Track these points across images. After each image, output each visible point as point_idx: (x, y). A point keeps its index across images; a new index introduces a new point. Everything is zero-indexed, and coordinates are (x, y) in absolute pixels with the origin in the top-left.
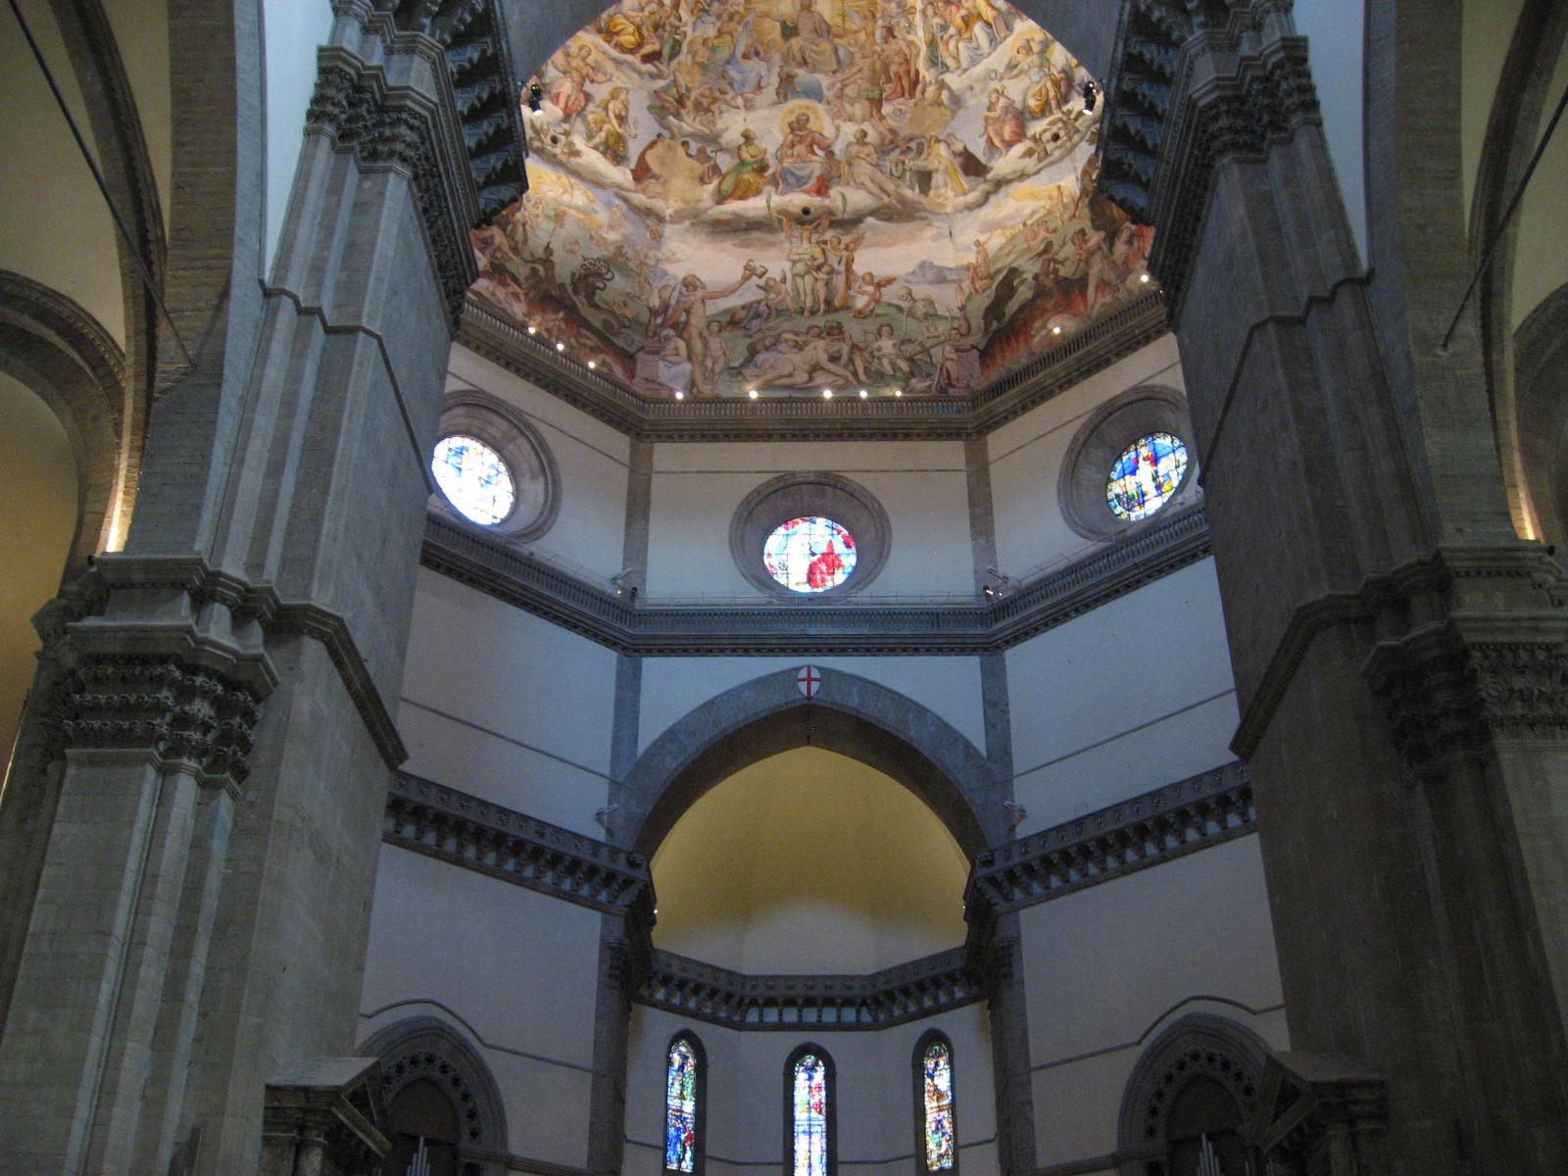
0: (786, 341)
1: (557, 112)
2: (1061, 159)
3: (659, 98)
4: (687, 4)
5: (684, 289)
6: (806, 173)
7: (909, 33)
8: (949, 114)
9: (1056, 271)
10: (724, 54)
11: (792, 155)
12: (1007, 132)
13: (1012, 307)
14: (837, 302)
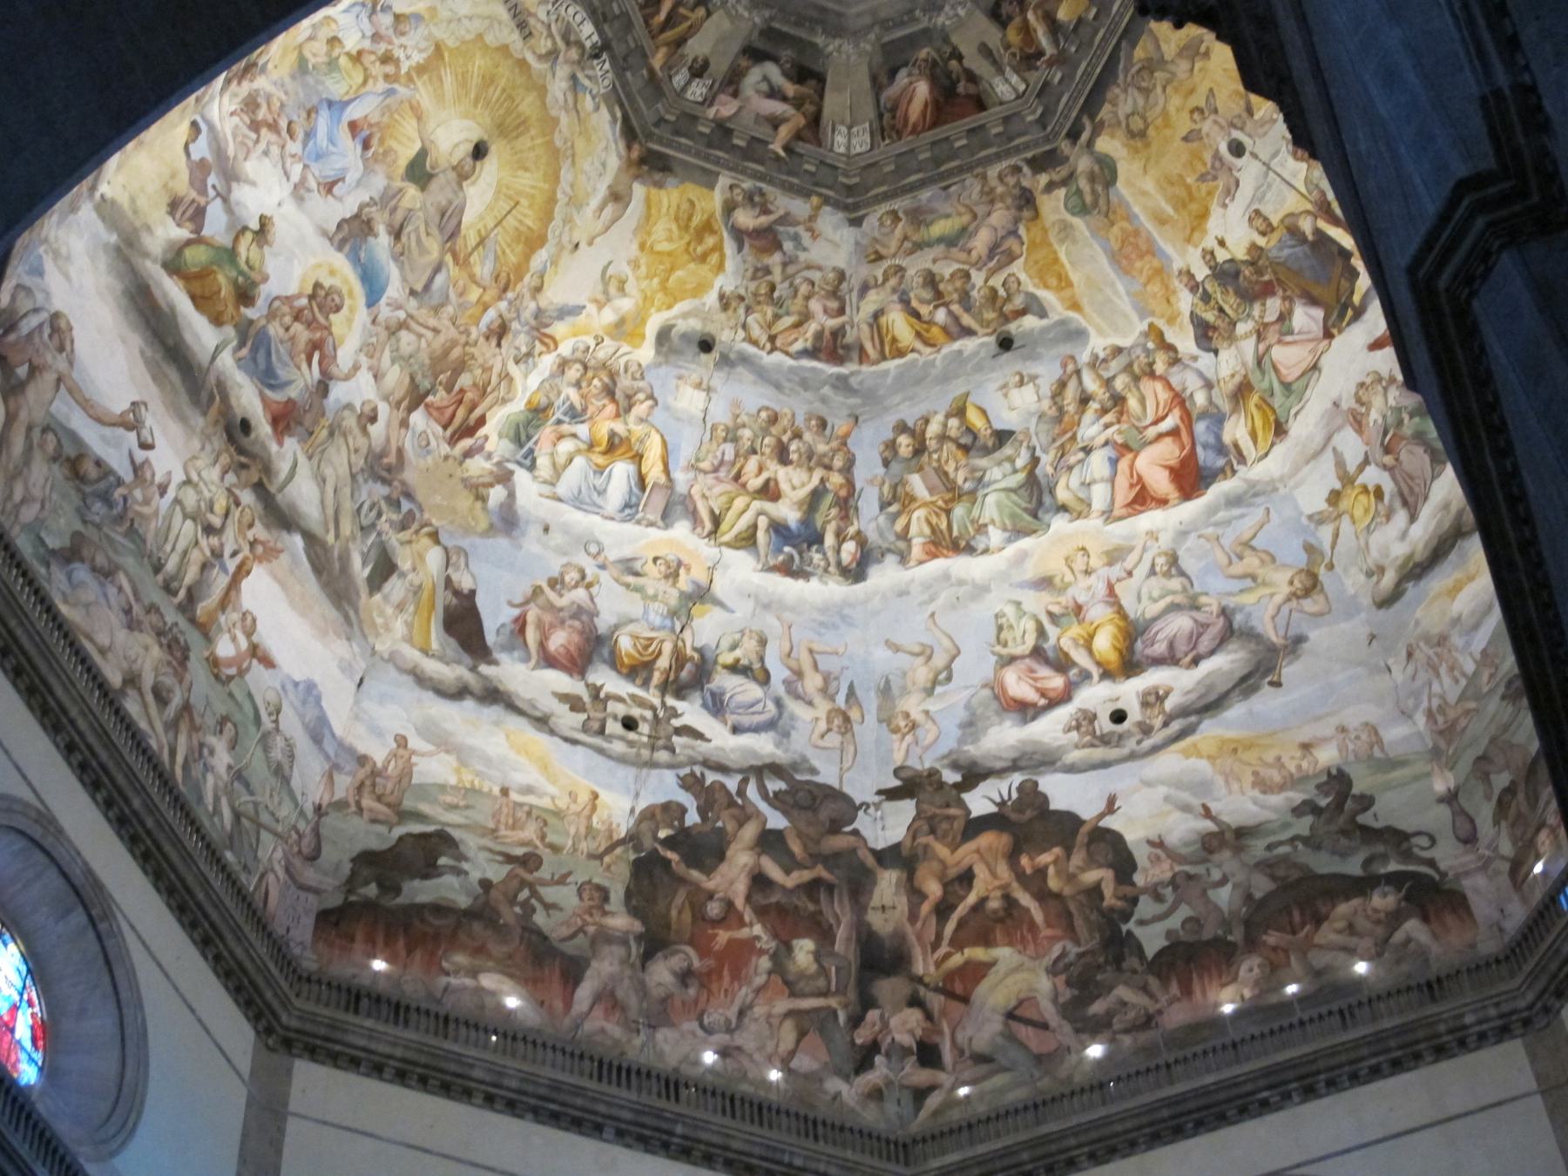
0: (120, 589)
2: (622, 760)
5: (47, 331)
6: (282, 373)
7: (517, 362)
8: (483, 525)
9: (529, 910)
10: (337, 88)
11: (287, 329)
12: (559, 641)
13: (420, 891)
14: (202, 608)
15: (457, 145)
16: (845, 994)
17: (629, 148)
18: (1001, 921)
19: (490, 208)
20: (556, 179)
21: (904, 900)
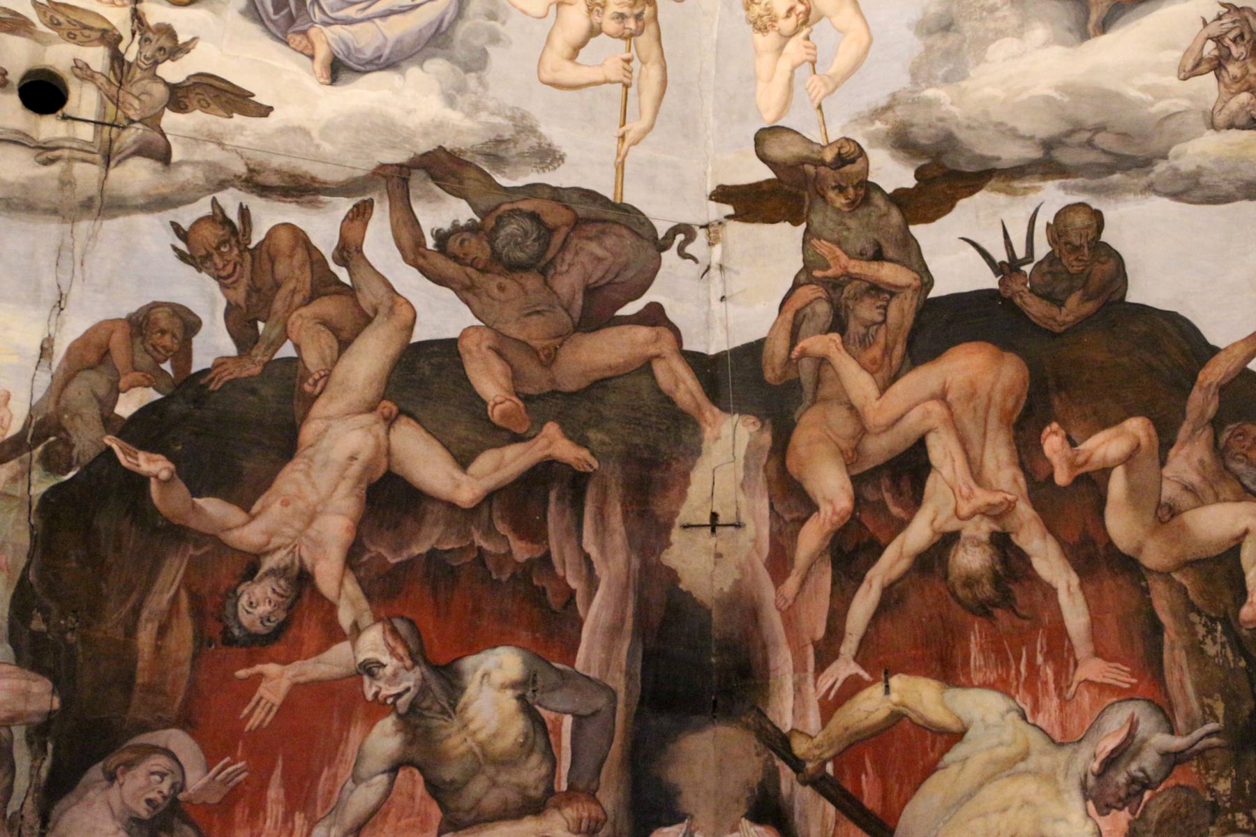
16: (592, 796)
18: (984, 610)
21: (763, 505)
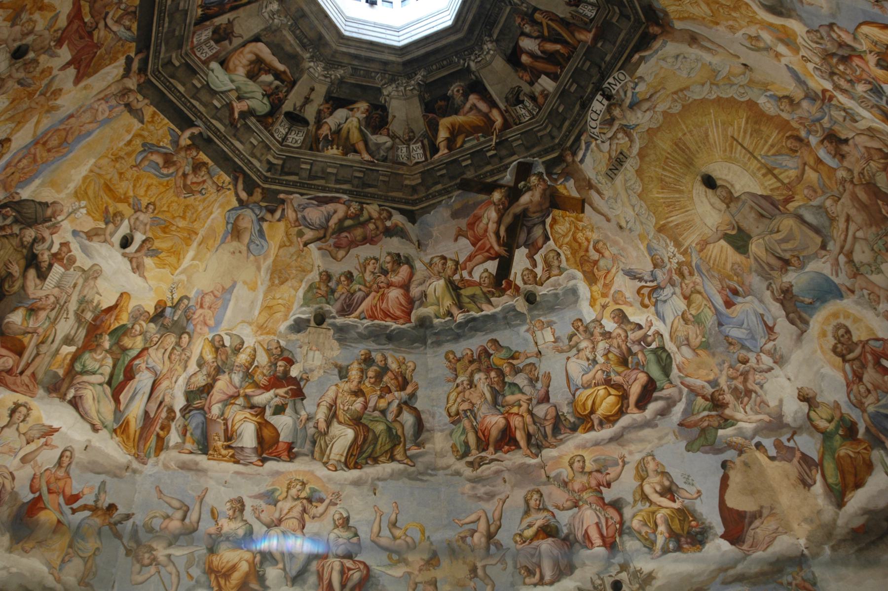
1: (600, 550)
3: (688, 427)
4: (631, 306)
7: (857, 122)
10: (710, 319)
15: (711, 205)
17: (655, 37)
19: (744, 167)
20: (703, 101)
